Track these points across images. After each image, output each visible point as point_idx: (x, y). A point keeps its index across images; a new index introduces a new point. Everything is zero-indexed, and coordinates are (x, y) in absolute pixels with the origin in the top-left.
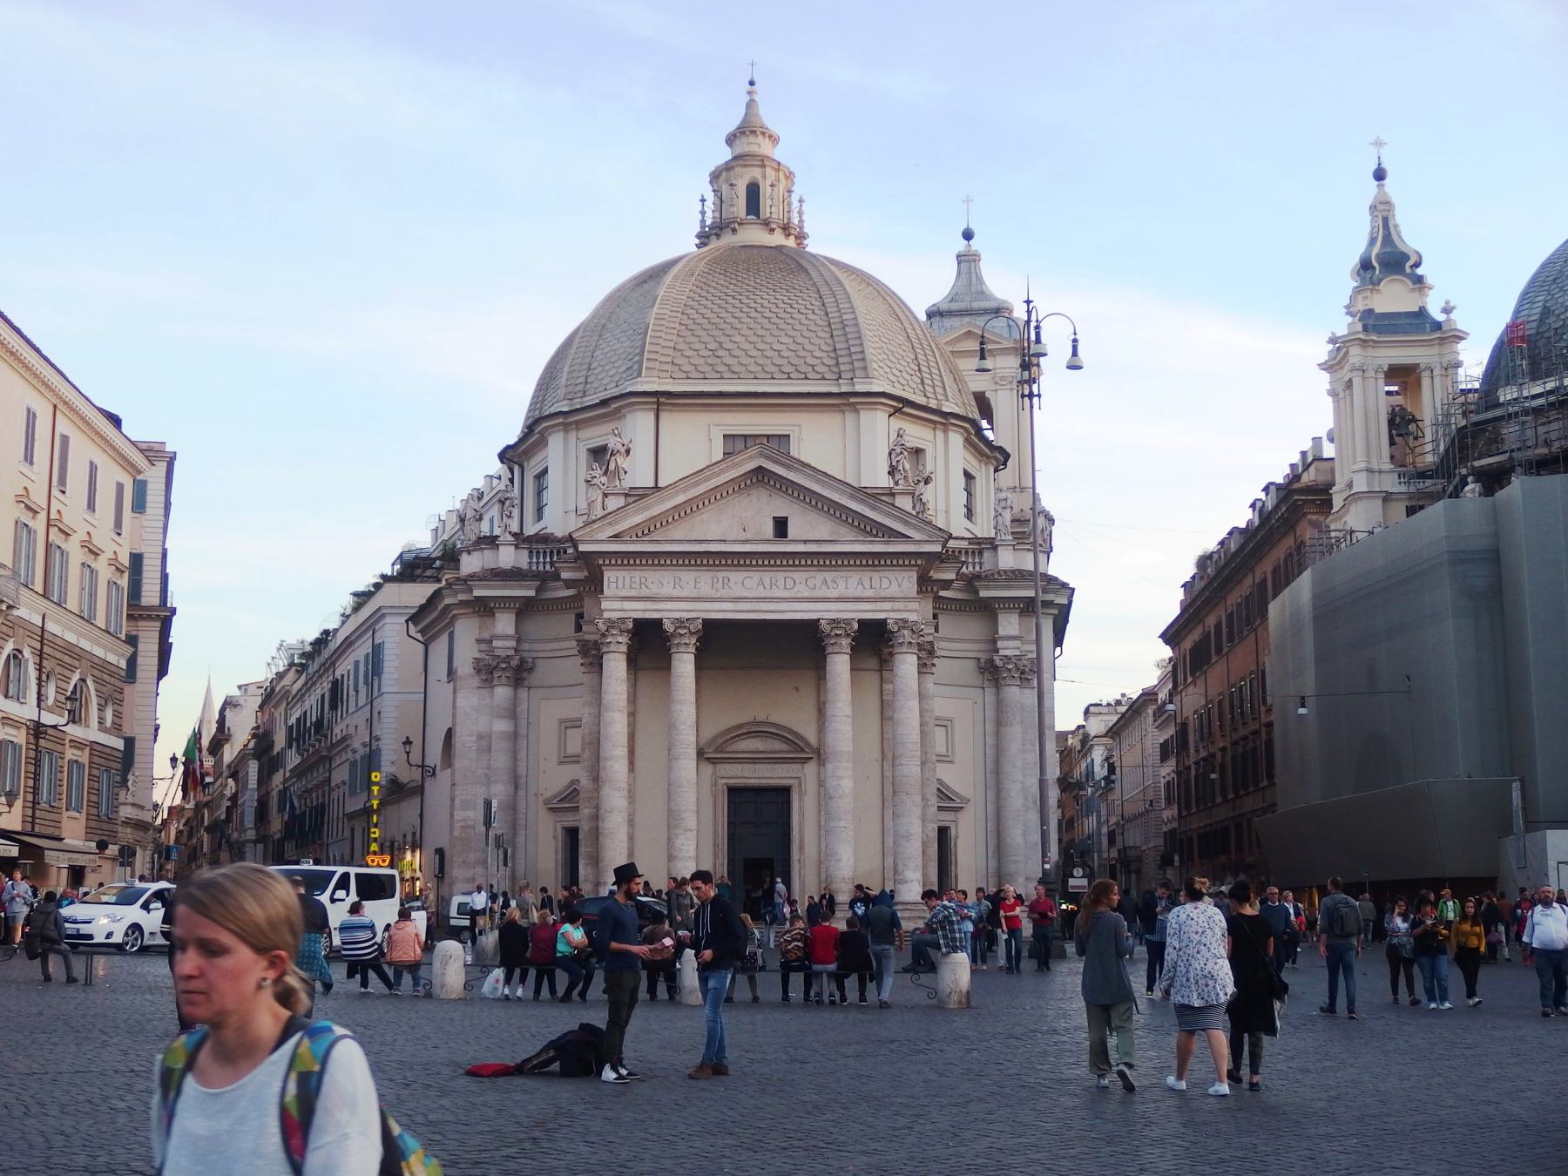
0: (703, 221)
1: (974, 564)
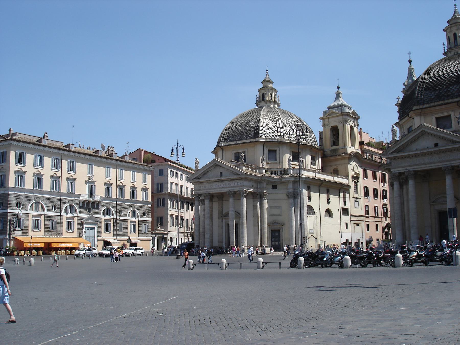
0: (444, 50)
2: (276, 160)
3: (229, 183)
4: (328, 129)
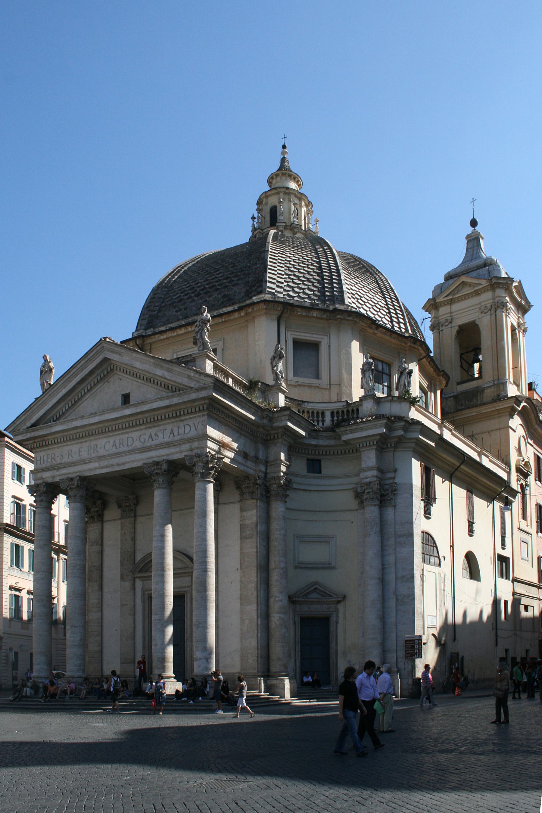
2: (318, 377)
3: (153, 431)
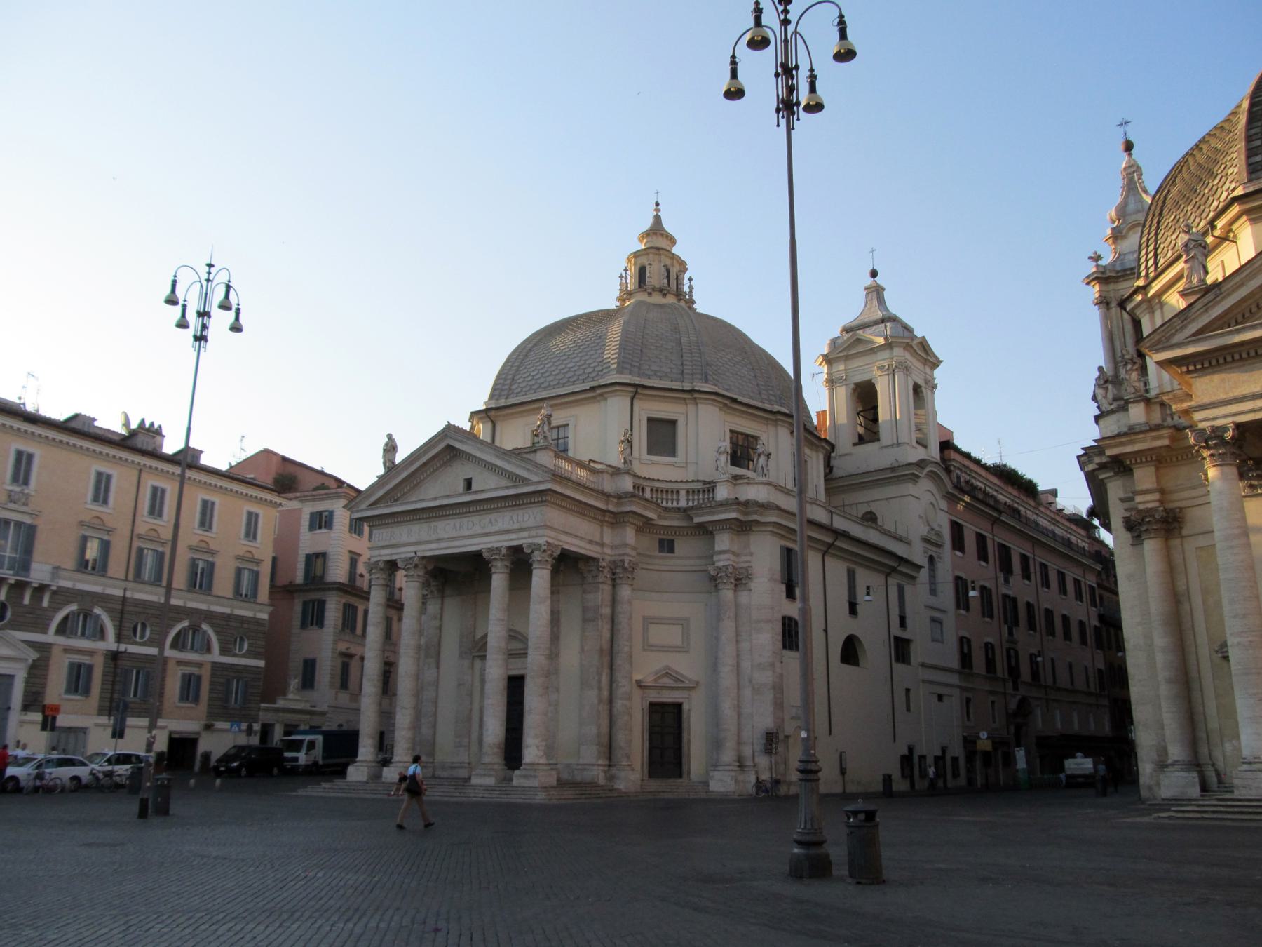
1: (693, 500)
4: (842, 393)
